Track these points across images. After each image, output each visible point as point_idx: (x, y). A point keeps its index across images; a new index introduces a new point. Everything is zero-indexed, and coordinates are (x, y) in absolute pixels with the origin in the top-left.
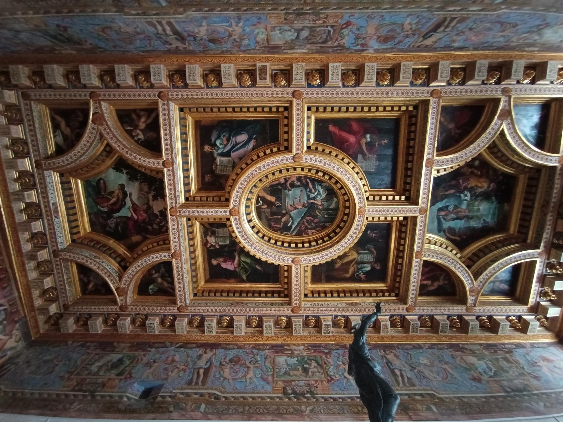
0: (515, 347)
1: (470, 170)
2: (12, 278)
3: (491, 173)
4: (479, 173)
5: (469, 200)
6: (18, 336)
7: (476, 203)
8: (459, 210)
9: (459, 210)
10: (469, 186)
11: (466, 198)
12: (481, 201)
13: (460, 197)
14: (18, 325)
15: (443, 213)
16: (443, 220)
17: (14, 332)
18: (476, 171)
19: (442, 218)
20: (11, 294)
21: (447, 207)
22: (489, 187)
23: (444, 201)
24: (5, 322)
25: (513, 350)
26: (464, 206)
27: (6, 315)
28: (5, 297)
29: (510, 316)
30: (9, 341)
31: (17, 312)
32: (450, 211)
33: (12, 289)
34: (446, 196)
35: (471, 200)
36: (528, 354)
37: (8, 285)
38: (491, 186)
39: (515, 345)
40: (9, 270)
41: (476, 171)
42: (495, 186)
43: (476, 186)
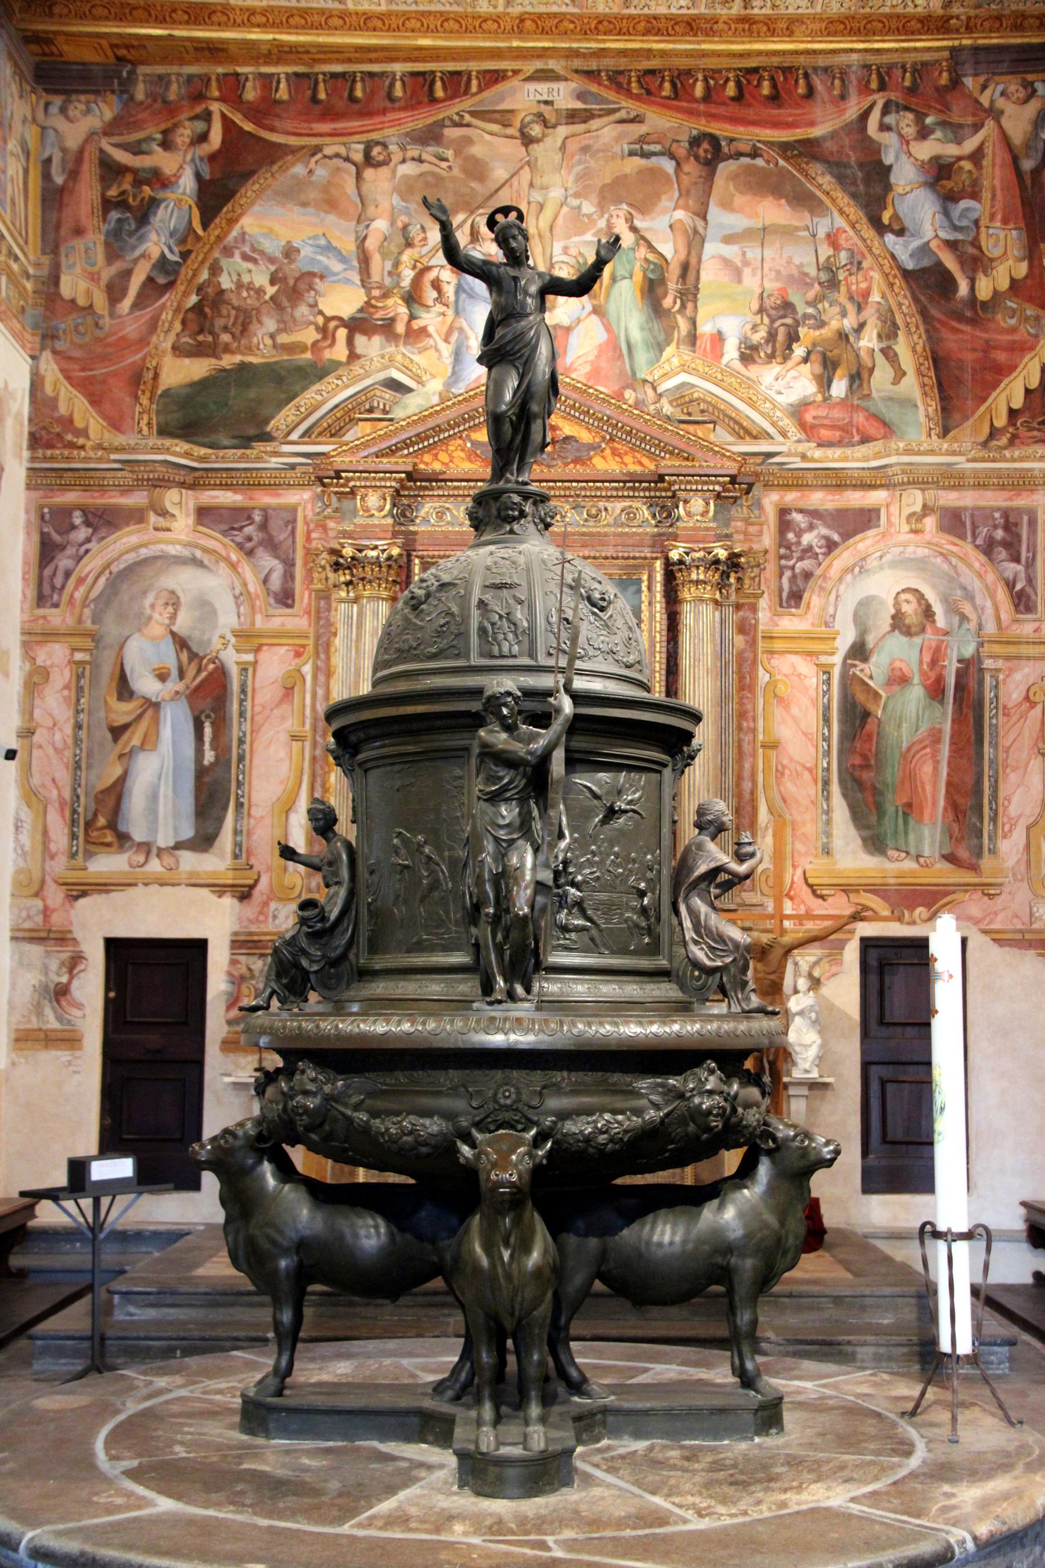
2: (787, 62)
6: (1012, 88)
14: (969, 82)
17: (985, 100)
20: (843, 74)
24: (929, 120)
27: (907, 108)
28: (843, 97)
30: (1004, 122)
31: (921, 70)
33: (826, 69)
37: (806, 76)
40: (752, 63)
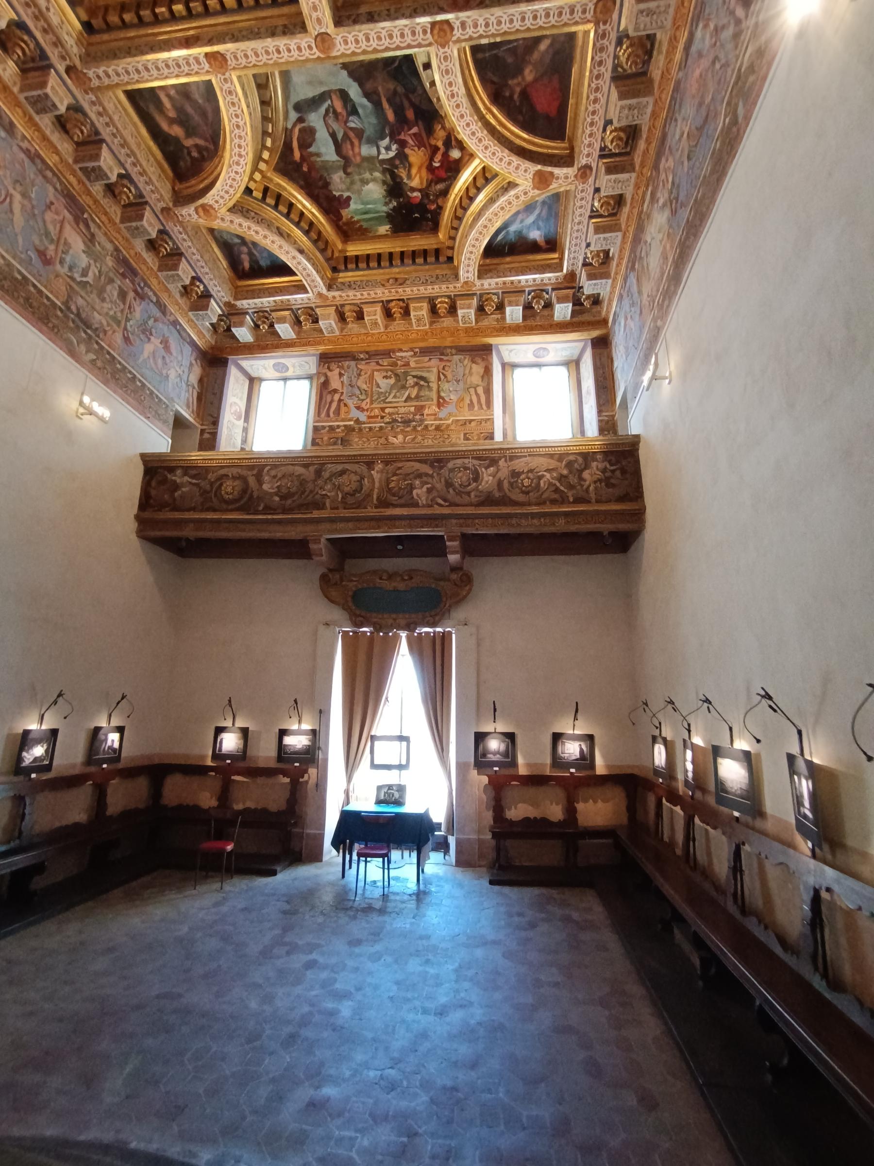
0: (155, 300)
1: (440, 144)
3: (440, 186)
4: (437, 165)
5: (381, 157)
7: (377, 174)
8: (356, 142)
9: (356, 142)
10: (407, 151)
11: (383, 151)
12: (384, 182)
13: (383, 138)
15: (338, 105)
16: (323, 110)
18: (438, 157)
19: (325, 106)
21: (354, 111)
22: (413, 190)
23: (365, 101)
25: (147, 300)
26: (366, 150)
29: (201, 281)
32: (346, 122)
34: (377, 104)
35: (383, 162)
36: (156, 320)
38: (415, 194)
39: (158, 301)
41: (438, 157)
42: (418, 201)
43: (410, 166)
